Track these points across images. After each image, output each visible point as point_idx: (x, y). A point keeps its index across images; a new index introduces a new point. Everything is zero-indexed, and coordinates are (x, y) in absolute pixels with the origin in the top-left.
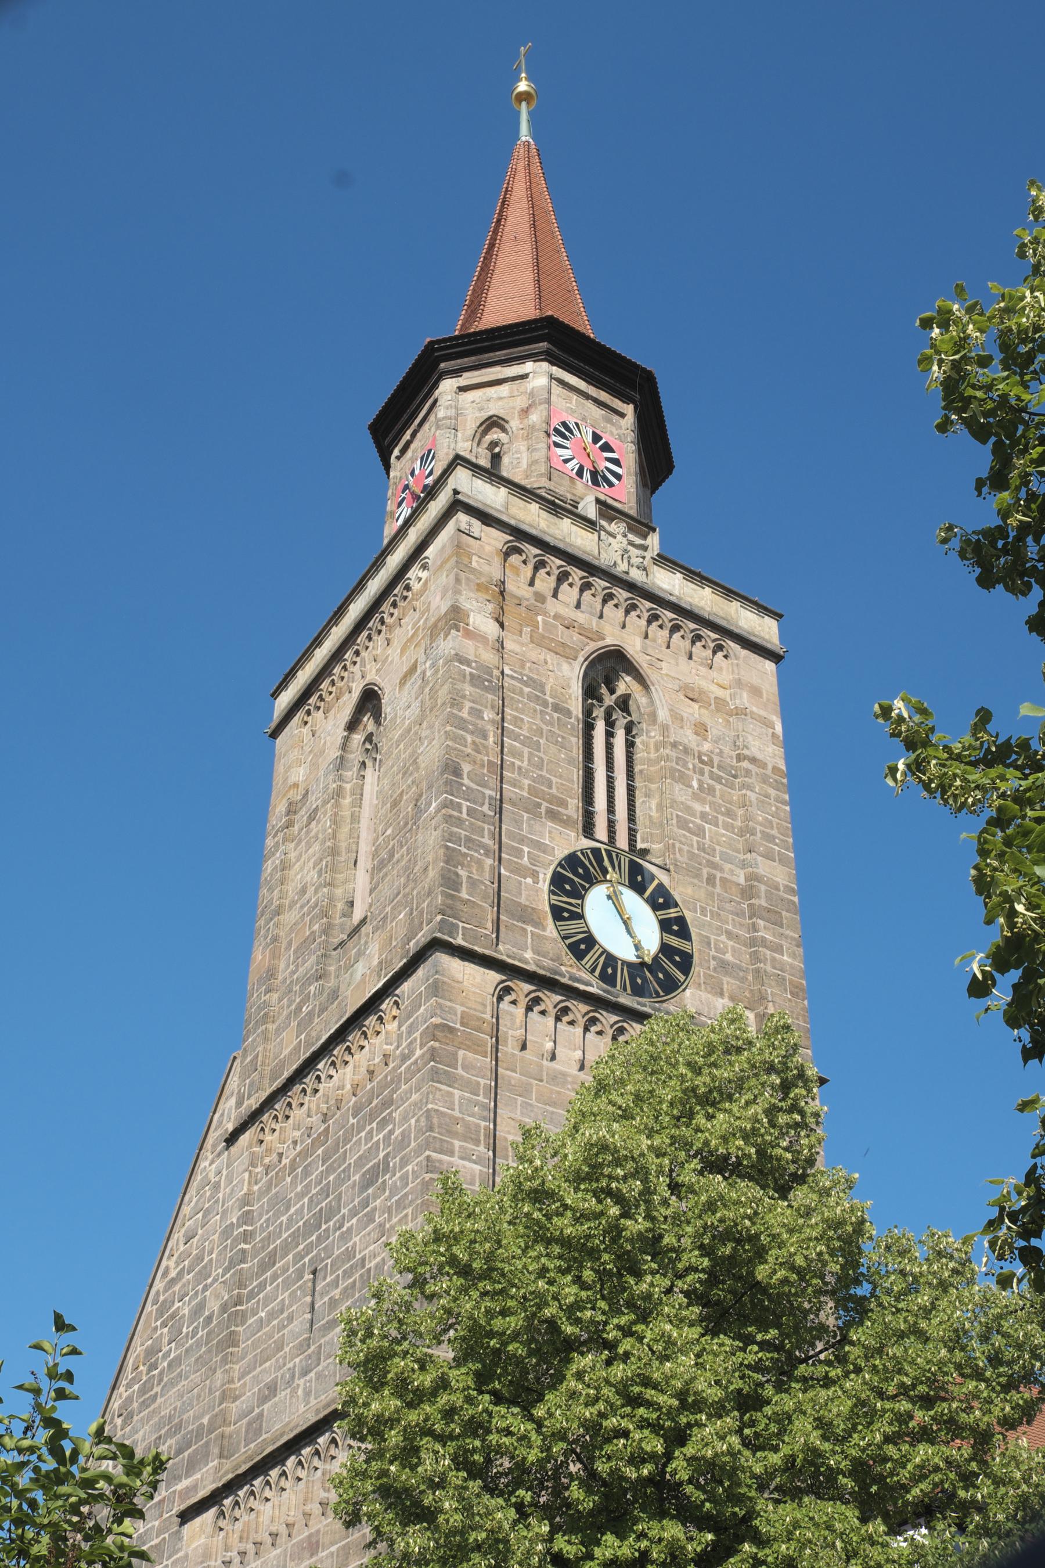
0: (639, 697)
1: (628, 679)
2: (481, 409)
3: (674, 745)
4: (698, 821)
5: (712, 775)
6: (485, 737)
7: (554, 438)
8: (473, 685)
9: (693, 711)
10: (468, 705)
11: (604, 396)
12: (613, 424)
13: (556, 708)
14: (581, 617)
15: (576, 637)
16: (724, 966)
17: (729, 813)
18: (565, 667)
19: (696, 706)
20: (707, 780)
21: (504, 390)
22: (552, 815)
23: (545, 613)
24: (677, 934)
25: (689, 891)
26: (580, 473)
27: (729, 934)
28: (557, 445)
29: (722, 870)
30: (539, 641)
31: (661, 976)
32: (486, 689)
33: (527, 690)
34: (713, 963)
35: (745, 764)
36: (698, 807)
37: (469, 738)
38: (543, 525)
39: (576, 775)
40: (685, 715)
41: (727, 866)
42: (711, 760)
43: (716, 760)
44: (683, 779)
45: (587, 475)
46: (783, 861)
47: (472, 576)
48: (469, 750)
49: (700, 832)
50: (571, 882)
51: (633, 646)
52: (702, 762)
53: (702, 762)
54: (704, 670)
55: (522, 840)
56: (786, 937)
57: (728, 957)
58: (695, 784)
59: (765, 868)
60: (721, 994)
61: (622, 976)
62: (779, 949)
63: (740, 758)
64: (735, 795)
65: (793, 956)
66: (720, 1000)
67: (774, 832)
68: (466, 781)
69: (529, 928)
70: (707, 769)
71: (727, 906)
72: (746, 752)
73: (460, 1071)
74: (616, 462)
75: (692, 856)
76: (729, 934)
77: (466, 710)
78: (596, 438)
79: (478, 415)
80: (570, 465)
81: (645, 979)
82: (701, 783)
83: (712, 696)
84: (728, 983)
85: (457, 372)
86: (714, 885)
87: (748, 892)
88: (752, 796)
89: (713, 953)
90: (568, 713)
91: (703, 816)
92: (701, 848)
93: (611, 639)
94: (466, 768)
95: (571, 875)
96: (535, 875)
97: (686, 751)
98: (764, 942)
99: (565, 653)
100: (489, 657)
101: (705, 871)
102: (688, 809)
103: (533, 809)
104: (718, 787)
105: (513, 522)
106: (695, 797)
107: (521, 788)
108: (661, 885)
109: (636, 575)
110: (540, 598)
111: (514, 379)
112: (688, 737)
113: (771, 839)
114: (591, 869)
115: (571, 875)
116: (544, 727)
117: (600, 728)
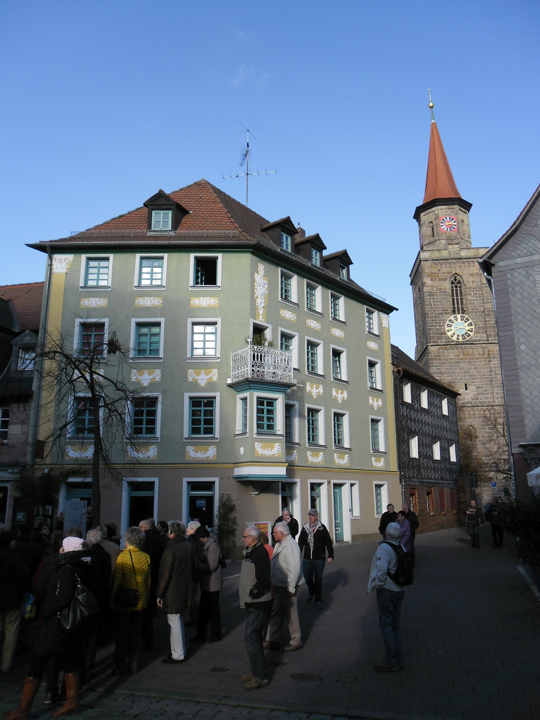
0: (461, 280)
1: (459, 277)
2: (428, 220)
3: (468, 288)
4: (473, 301)
5: (476, 291)
6: (432, 305)
7: (441, 225)
8: (428, 296)
9: (471, 279)
10: (428, 300)
11: (450, 206)
12: (453, 212)
13: (444, 292)
14: (448, 270)
15: (447, 274)
16: (479, 328)
17: (480, 297)
18: (445, 282)
19: (471, 277)
20: (475, 292)
21: (431, 214)
22: (446, 313)
23: (440, 273)
24: (469, 326)
25: (472, 316)
26: (447, 230)
27: (481, 321)
28: (442, 226)
29: (479, 309)
30: (440, 280)
31: (467, 335)
32: (431, 296)
33: (438, 291)
34: (477, 328)
35: (483, 285)
36: (473, 299)
37: (429, 307)
38: (438, 255)
39: (451, 301)
40: (469, 280)
41: (479, 308)
42: (475, 287)
43: (476, 287)
44: (470, 294)
45: (449, 230)
46: (491, 302)
47: (425, 274)
48: (429, 309)
49: (474, 303)
50: (450, 325)
51: (458, 271)
52: (473, 289)
53: (473, 289)
54: (473, 268)
55: (441, 320)
56: (491, 318)
57: (481, 326)
58: (472, 294)
59: (487, 306)
60: (479, 333)
61: (461, 338)
62: (490, 321)
63: (481, 284)
64: (481, 292)
65: (493, 321)
66: (479, 335)
67: (489, 297)
68: (430, 315)
69: (443, 336)
70: (475, 290)
71: (480, 316)
72: (482, 283)
73: (434, 364)
74: (455, 222)
75: (472, 309)
76: (481, 321)
77: (428, 302)
78: (450, 218)
79: (428, 221)
80: (445, 229)
81: (464, 336)
82: (473, 293)
83: (475, 273)
84: (480, 331)
85: (422, 212)
86: (477, 313)
87: (484, 312)
88: (484, 292)
89: (477, 326)
90: (447, 292)
91: (474, 300)
92: (474, 307)
93: (454, 272)
94: (429, 312)
95: (450, 323)
96: (444, 326)
97: (470, 288)
98: (487, 321)
99: (445, 279)
100: (430, 289)
101: (475, 311)
102: (471, 300)
103: (442, 314)
104: (477, 292)
105: (431, 259)
106: (473, 297)
107: (440, 311)
108: (467, 318)
109: (457, 256)
110: (439, 270)
111: (432, 212)
112: (470, 285)
113: (488, 299)
114: (453, 321)
115: (450, 323)
116: (443, 297)
117: (454, 289)
